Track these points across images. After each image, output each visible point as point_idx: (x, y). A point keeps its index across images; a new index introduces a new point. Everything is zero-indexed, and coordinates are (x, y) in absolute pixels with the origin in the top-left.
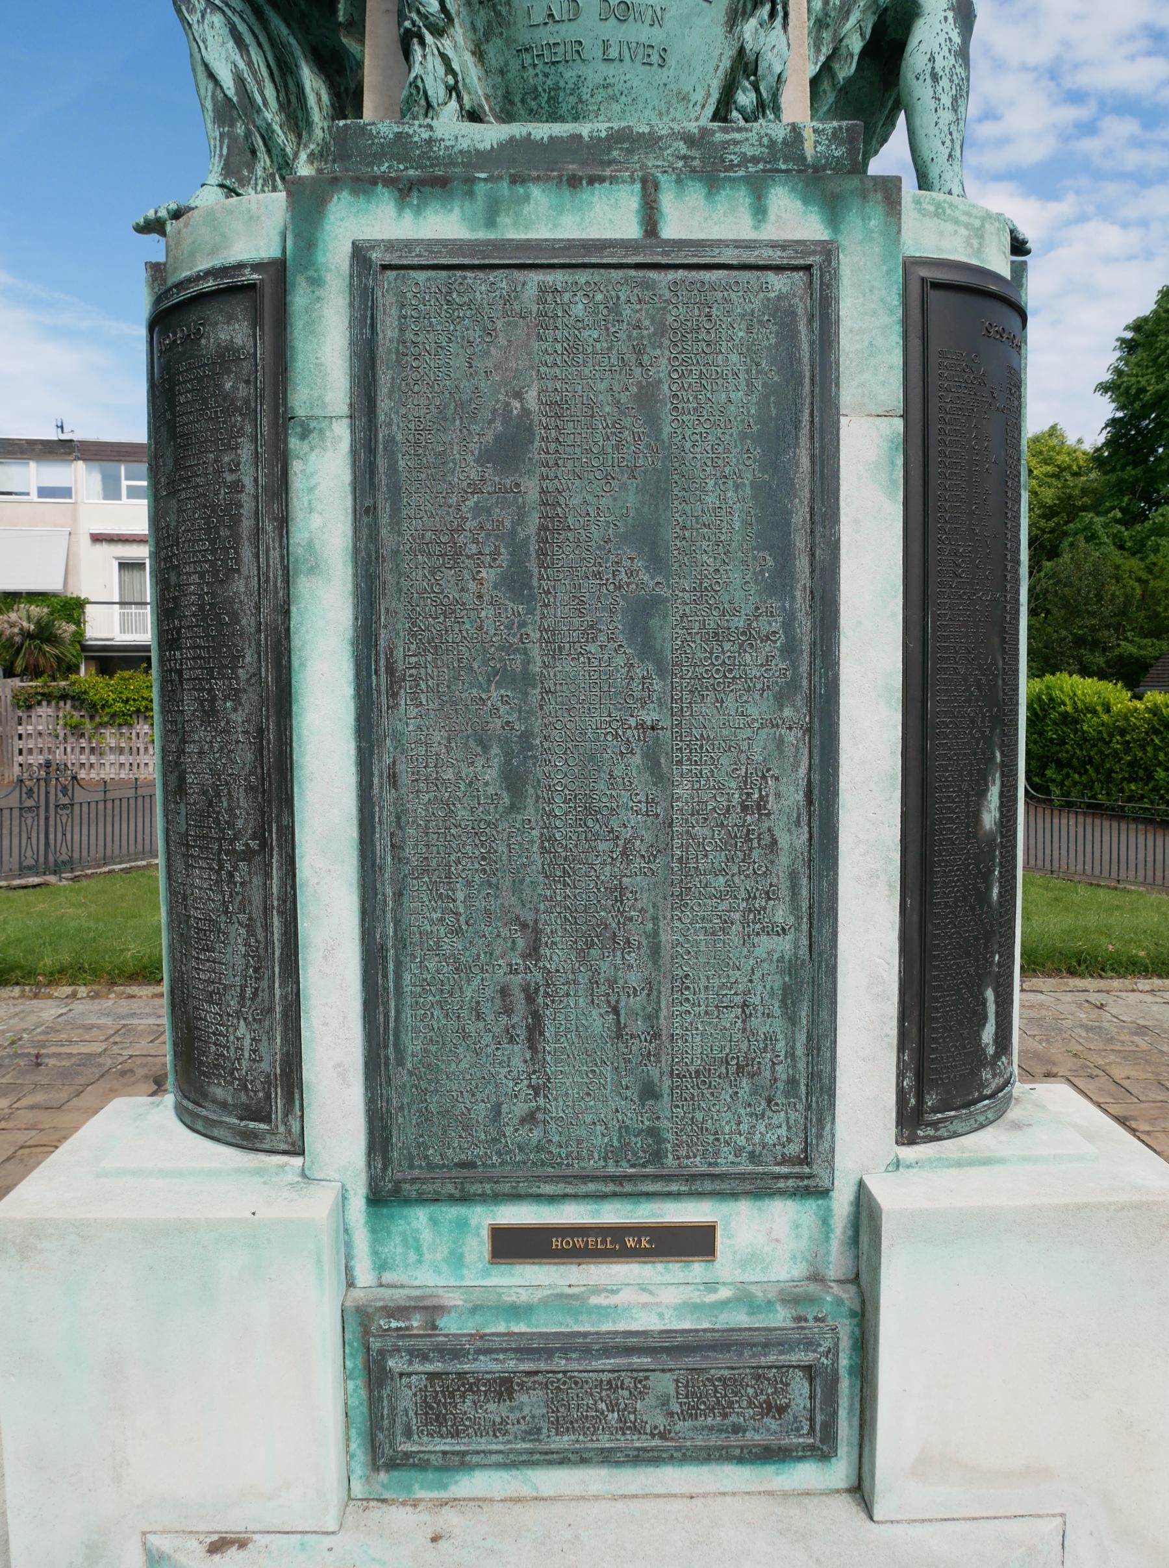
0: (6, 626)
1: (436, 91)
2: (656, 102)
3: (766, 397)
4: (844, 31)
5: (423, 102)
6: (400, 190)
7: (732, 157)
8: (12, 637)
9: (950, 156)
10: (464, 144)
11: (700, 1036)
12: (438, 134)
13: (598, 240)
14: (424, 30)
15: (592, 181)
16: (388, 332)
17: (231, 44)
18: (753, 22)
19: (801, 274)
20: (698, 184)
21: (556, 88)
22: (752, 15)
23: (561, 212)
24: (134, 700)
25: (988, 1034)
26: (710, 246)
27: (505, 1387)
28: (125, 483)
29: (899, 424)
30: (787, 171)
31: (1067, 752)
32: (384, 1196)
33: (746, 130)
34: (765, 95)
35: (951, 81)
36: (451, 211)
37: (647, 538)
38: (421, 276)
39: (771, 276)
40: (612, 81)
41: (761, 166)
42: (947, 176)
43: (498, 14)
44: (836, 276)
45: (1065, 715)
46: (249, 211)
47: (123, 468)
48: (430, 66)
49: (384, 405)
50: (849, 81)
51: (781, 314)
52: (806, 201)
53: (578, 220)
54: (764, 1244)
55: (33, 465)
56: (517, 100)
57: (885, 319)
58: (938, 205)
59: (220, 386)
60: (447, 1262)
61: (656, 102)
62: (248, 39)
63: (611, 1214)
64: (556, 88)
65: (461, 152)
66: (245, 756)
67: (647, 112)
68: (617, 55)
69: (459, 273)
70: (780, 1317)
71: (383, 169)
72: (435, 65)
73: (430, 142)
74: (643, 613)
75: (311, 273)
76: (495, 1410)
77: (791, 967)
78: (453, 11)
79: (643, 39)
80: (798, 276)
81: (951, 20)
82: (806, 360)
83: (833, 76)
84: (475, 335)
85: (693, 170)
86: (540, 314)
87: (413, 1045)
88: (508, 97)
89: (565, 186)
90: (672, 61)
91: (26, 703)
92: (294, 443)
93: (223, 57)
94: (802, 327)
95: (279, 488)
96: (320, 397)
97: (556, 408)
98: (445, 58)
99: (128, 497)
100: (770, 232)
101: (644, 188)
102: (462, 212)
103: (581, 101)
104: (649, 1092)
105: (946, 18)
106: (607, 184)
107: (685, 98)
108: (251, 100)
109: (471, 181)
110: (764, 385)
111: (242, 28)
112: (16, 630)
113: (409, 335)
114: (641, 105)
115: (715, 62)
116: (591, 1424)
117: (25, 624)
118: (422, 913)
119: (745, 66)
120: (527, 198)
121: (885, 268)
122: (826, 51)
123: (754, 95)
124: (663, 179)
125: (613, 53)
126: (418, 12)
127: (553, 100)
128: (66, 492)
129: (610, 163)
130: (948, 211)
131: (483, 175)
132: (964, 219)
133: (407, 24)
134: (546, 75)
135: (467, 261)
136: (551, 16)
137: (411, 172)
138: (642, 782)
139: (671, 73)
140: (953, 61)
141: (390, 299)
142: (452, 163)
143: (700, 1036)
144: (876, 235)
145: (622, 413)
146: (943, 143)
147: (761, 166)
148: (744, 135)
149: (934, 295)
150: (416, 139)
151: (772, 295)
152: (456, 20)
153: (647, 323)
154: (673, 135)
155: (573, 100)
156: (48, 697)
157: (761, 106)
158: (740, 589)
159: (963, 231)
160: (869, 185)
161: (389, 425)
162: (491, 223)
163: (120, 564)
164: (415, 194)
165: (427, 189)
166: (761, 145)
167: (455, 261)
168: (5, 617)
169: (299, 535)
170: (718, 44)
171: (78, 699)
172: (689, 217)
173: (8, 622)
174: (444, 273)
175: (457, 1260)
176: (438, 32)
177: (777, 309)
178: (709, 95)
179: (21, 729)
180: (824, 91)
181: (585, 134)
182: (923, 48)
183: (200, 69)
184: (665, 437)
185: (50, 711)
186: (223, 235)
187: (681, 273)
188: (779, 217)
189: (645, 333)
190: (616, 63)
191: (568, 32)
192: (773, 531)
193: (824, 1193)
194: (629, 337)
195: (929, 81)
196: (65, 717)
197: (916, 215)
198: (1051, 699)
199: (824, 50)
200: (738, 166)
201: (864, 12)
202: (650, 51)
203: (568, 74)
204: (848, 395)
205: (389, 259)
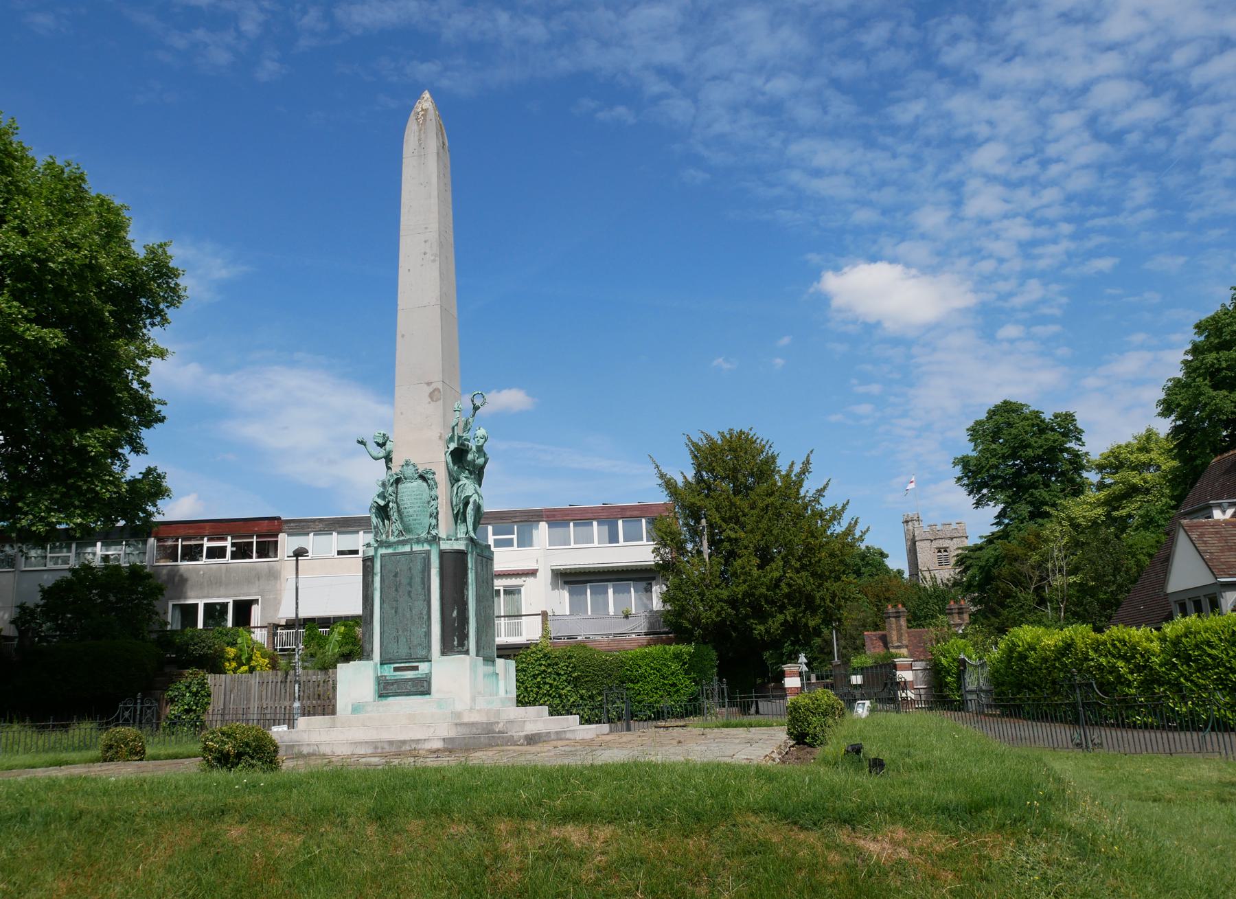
37: (410, 584)
45: (1019, 653)
60: (388, 672)
143: (415, 641)
192: (423, 583)
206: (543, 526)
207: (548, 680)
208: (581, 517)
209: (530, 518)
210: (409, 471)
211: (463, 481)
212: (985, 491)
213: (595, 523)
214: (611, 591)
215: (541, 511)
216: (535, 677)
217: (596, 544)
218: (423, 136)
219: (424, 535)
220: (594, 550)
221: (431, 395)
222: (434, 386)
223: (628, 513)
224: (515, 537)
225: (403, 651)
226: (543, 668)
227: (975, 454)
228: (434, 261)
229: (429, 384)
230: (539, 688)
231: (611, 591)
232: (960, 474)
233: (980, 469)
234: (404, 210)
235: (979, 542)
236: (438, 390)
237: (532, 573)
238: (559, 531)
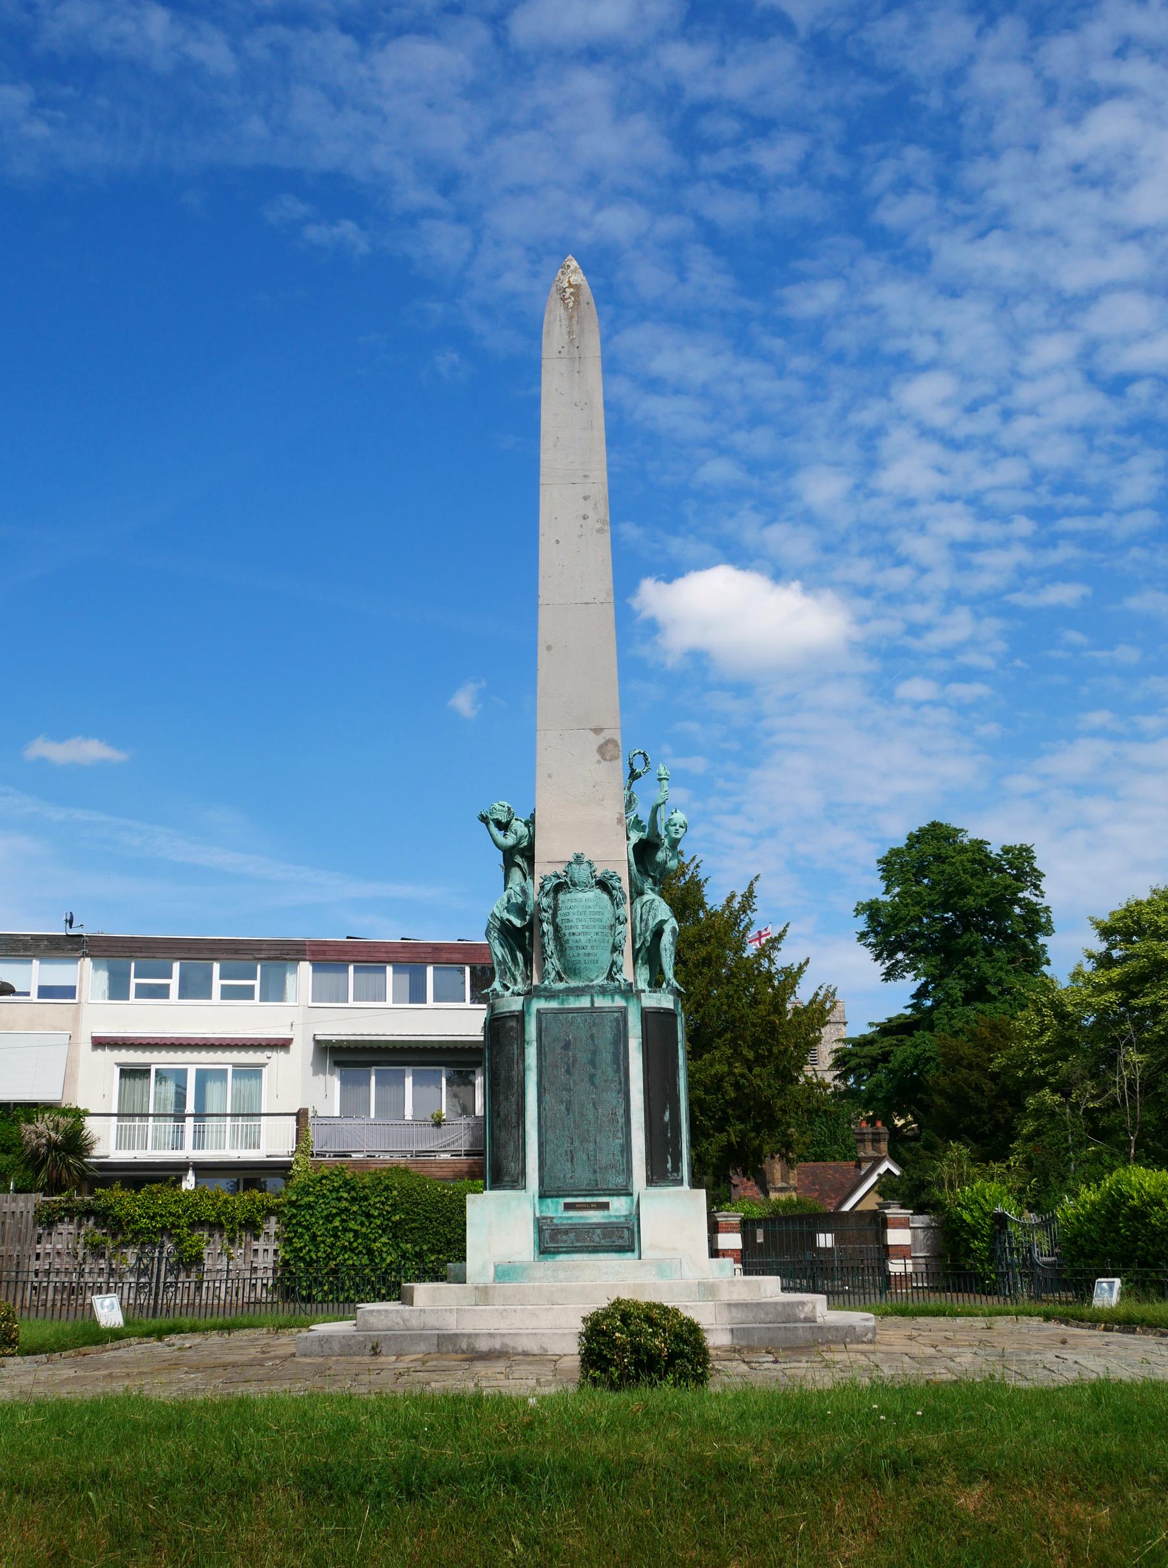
0: (33, 1136)
8: (39, 1146)
11: (604, 1159)
24: (161, 1216)
25: (669, 1165)
27: (566, 1232)
28: (134, 981)
31: (1142, 1249)
32: (542, 1196)
37: (592, 1063)
45: (1133, 1209)
47: (133, 965)
51: (617, 1020)
54: (619, 1206)
55: (36, 963)
60: (555, 1209)
63: (588, 1200)
66: (514, 1107)
70: (622, 1220)
74: (592, 1077)
76: (565, 1237)
77: (622, 1146)
87: (548, 1162)
91: (48, 1221)
95: (522, 1054)
97: (575, 1039)
99: (137, 997)
100: (615, 1005)
104: (595, 1172)
112: (44, 1141)
116: (584, 1240)
117: (53, 1134)
118: (550, 1136)
119: (614, 963)
128: (68, 992)
138: (592, 1109)
143: (604, 1159)
156: (70, 1213)
158: (610, 1072)
163: (122, 1071)
168: (32, 1127)
169: (527, 1063)
171: (102, 1216)
172: (600, 1002)
173: (36, 1132)
175: (556, 1210)
179: (39, 1248)
185: (72, 1228)
193: (631, 1194)
196: (86, 1235)
198: (1122, 1195)
204: (631, 1034)
206: (305, 968)
207: (352, 1225)
208: (367, 957)
209: (283, 954)
210: (581, 873)
211: (650, 896)
212: (900, 956)
213: (389, 969)
214: (409, 1081)
215: (303, 943)
216: (329, 1218)
217: (389, 1003)
218: (575, 327)
219: (600, 981)
220: (387, 1016)
221: (601, 750)
222: (607, 735)
223: (445, 956)
224: (257, 983)
225: (583, 1176)
226: (345, 1204)
227: (887, 898)
228: (600, 531)
230: (336, 1236)
231: (409, 1081)
232: (864, 928)
233: (896, 920)
234: (546, 442)
235: (868, 1031)
237: (283, 1045)
238: (330, 978)
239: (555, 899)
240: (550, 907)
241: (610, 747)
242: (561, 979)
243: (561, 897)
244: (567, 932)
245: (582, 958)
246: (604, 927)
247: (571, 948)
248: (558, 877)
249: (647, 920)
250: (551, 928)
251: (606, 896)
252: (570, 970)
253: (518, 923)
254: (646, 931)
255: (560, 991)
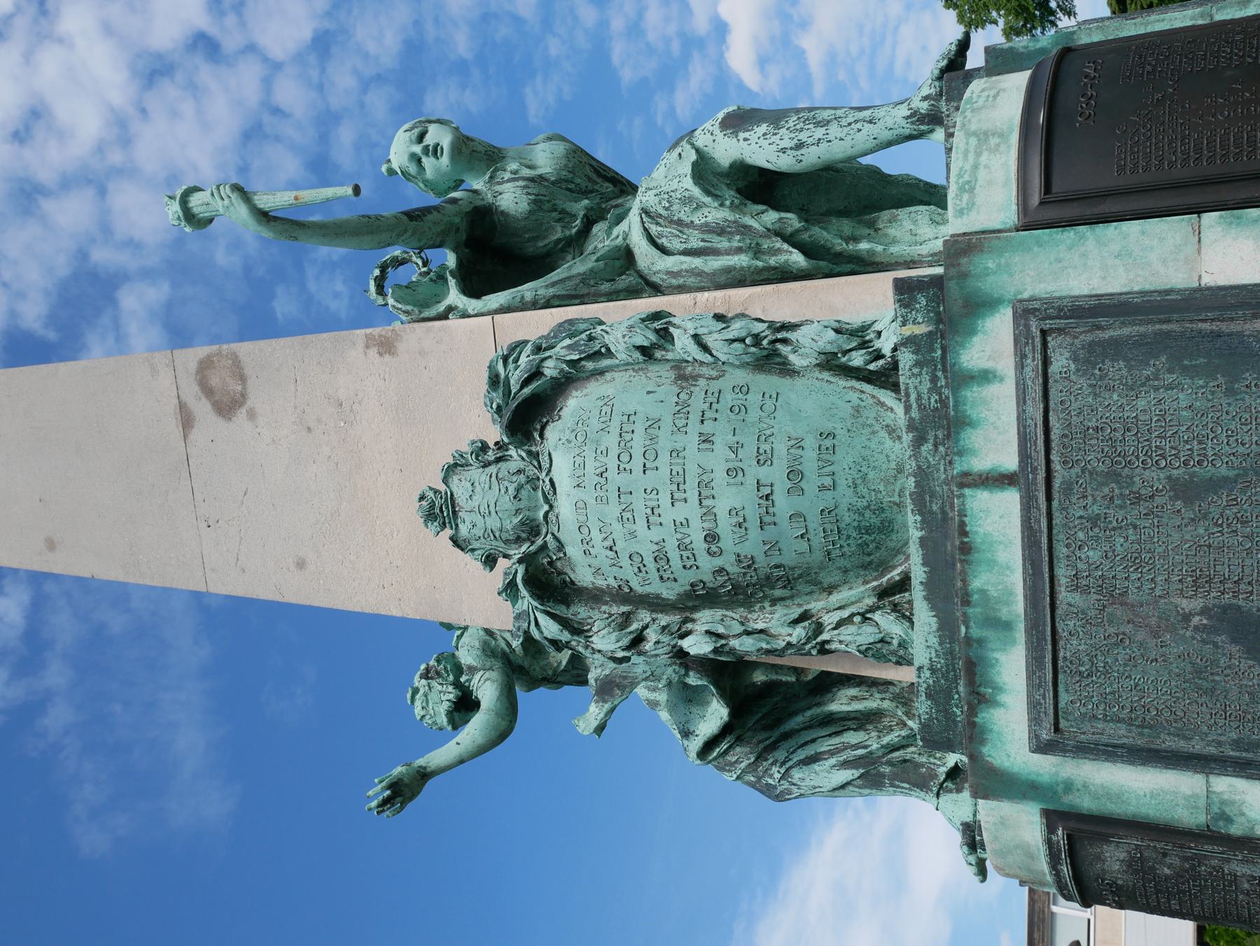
1: (867, 635)
2: (864, 438)
3: (1185, 370)
4: (761, 228)
5: (879, 646)
6: (979, 702)
7: (932, 400)
9: (870, 122)
10: (934, 641)
12: (926, 662)
13: (1023, 532)
14: (819, 639)
15: (964, 533)
16: (1121, 734)
17: (816, 767)
18: (792, 358)
19: (1049, 339)
20: (962, 435)
21: (858, 528)
22: (786, 358)
23: (995, 562)
26: (1025, 427)
29: (1209, 218)
30: (944, 349)
33: (907, 389)
34: (854, 344)
35: (802, 130)
36: (997, 660)
38: (1064, 698)
39: (1054, 368)
40: (850, 480)
41: (940, 374)
42: (890, 124)
43: (800, 576)
44: (1049, 302)
46: (995, 824)
48: (849, 638)
49: (1197, 746)
50: (801, 219)
51: (1090, 357)
52: (972, 332)
53: (1001, 547)
56: (868, 559)
57: (1090, 243)
58: (962, 189)
59: (1167, 878)
61: (864, 438)
62: (809, 751)
64: (858, 528)
65: (940, 644)
67: (873, 446)
68: (829, 479)
69: (1061, 663)
71: (959, 713)
72: (847, 632)
73: (933, 670)
75: (1060, 789)
78: (800, 611)
79: (814, 455)
80: (1052, 343)
81: (746, 135)
82: (1142, 329)
83: (798, 231)
84: (1122, 654)
85: (948, 436)
86: (1099, 593)
88: (866, 566)
89: (970, 557)
90: (828, 426)
92: (1235, 830)
93: (828, 775)
94: (1107, 335)
96: (1187, 798)
97: (1199, 582)
98: (839, 625)
100: (1006, 365)
101: (969, 486)
102: (997, 650)
103: (868, 507)
105: (745, 140)
106: (967, 520)
107: (857, 409)
108: (861, 757)
109: (968, 640)
110: (1170, 371)
111: (801, 754)
113: (1124, 714)
114: (868, 452)
115: (824, 384)
119: (831, 363)
120: (983, 592)
121: (1036, 249)
122: (779, 244)
123: (854, 353)
124: (958, 468)
125: (828, 481)
126: (805, 644)
127: (868, 530)
129: (944, 513)
130: (966, 178)
131: (963, 629)
132: (971, 157)
133: (814, 652)
134: (849, 537)
135: (1049, 657)
136: (802, 536)
137: (961, 689)
139: (838, 426)
140: (784, 130)
141: (1087, 727)
142: (951, 652)
144: (1003, 261)
145: (1205, 517)
146: (859, 130)
147: (940, 374)
148: (912, 390)
149: (1056, 187)
150: (931, 682)
151: (1073, 367)
152: (805, 607)
153: (1106, 490)
154: (916, 455)
155: (868, 514)
157: (864, 345)
159: (984, 158)
160: (953, 271)
161: (1220, 744)
162: (1007, 626)
164: (982, 690)
165: (978, 679)
166: (920, 374)
167: (1049, 666)
170: (809, 382)
172: (995, 440)
174: (1061, 677)
176: (819, 628)
177: (1087, 361)
178: (852, 388)
180: (811, 236)
181: (919, 534)
182: (773, 159)
183: (836, 793)
184: (1232, 473)
186: (1017, 847)
187: (1055, 457)
188: (989, 358)
189: (1117, 491)
190: (836, 478)
191: (814, 522)
194: (1121, 507)
195: (803, 151)
197: (973, 214)
199: (778, 245)
200: (940, 395)
201: (745, 214)
202: (823, 447)
203: (847, 520)
204: (1176, 277)
205: (1048, 722)
210: (486, 500)
222: (191, 391)
229: (187, 421)
236: (205, 366)
239: (595, 596)
240: (627, 619)
241: (215, 381)
242: (904, 584)
243: (583, 576)
244: (707, 564)
245: (811, 503)
246: (682, 409)
247: (773, 546)
248: (510, 589)
249: (707, 229)
250: (706, 618)
251: (574, 404)
252: (865, 546)
253: (715, 714)
254: (745, 230)
255: (947, 628)
